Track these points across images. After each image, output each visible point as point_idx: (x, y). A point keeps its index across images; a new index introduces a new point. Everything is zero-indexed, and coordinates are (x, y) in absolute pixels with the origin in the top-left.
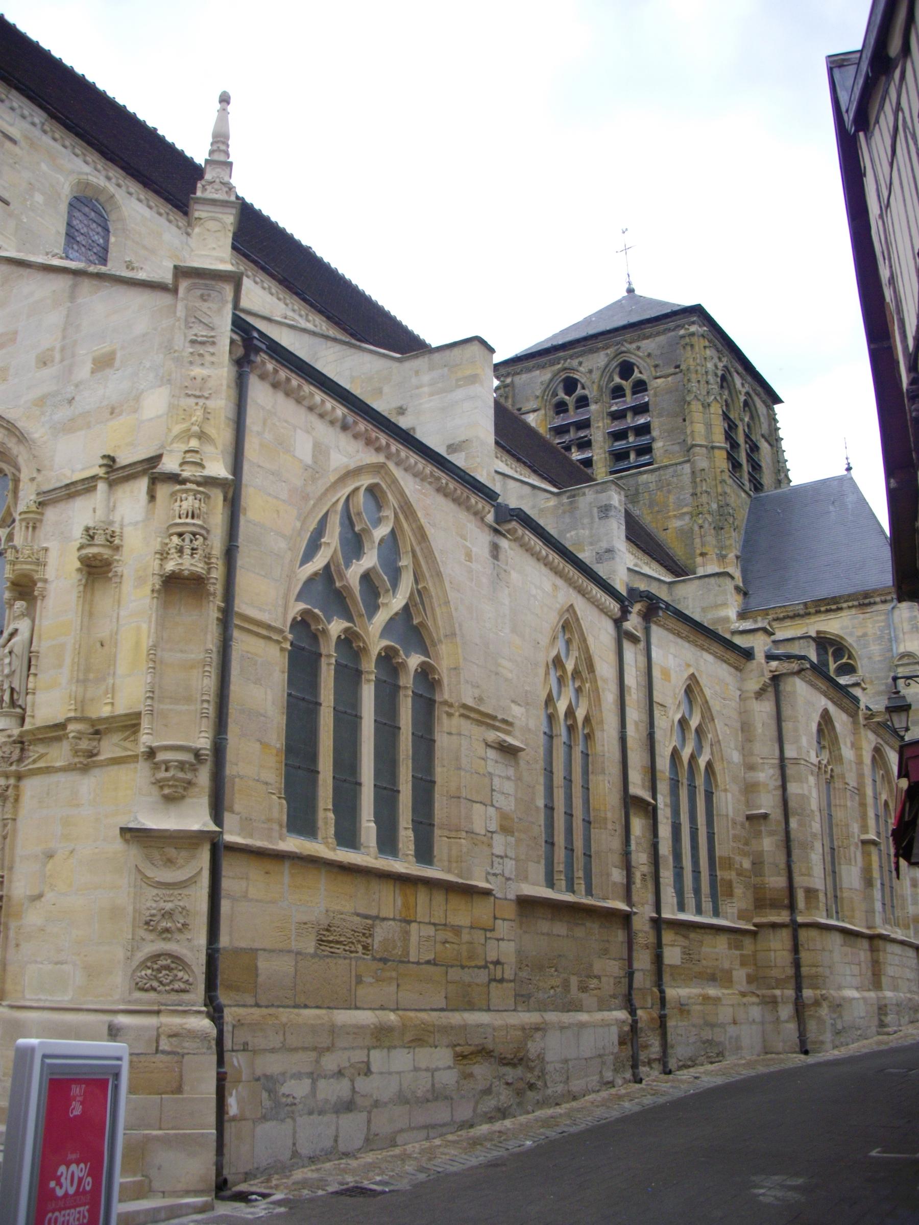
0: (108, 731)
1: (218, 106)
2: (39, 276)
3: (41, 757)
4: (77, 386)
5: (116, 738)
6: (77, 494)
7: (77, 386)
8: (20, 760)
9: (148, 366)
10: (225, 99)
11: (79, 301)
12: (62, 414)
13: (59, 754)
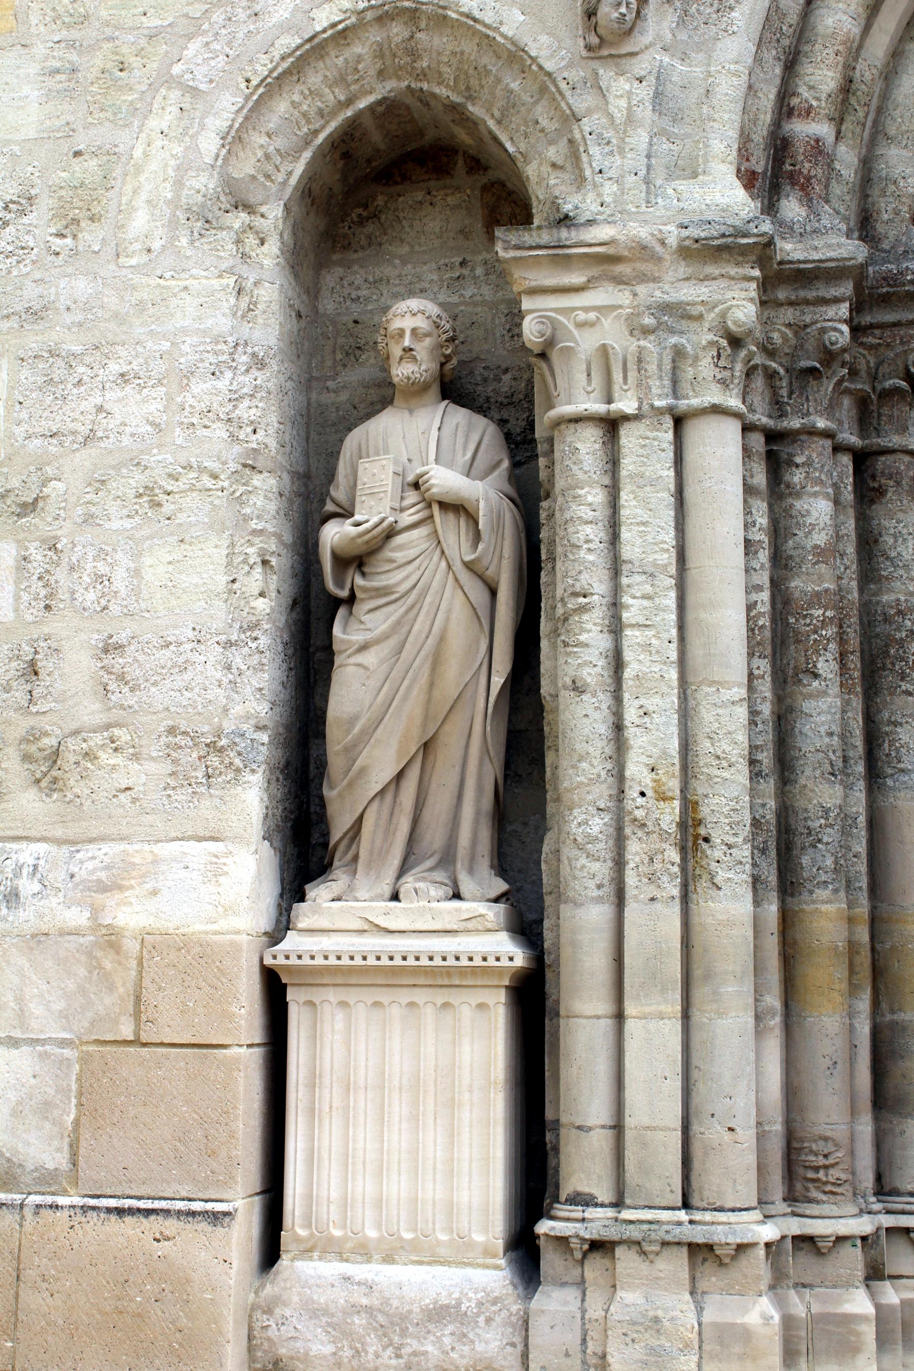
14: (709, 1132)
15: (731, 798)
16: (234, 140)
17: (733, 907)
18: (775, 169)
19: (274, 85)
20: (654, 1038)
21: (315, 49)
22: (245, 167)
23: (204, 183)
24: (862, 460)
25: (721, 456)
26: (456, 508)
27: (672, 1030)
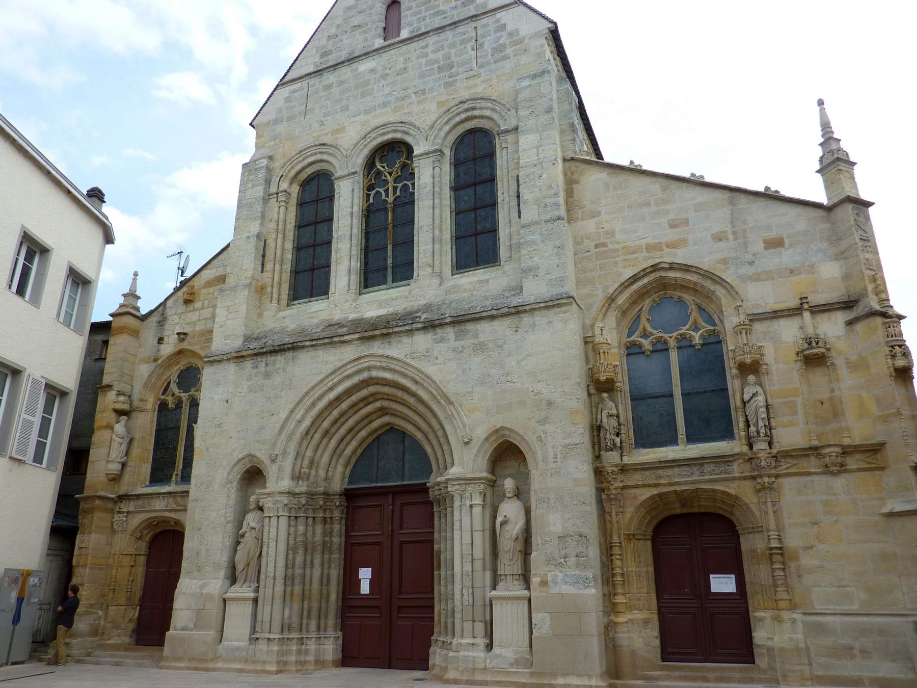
0: (851, 453)
1: (818, 108)
2: (698, 188)
3: (794, 465)
4: (754, 255)
5: (858, 456)
6: (783, 316)
7: (754, 255)
8: (775, 467)
9: (815, 248)
10: (821, 103)
11: (740, 206)
12: (751, 270)
13: (812, 464)
14: (273, 622)
15: (280, 572)
16: (229, 474)
17: (279, 588)
18: (297, 477)
19: (235, 466)
20: (268, 608)
21: (240, 460)
22: (231, 477)
23: (224, 480)
24: (314, 518)
25: (283, 521)
26: (254, 529)
27: (269, 607)
